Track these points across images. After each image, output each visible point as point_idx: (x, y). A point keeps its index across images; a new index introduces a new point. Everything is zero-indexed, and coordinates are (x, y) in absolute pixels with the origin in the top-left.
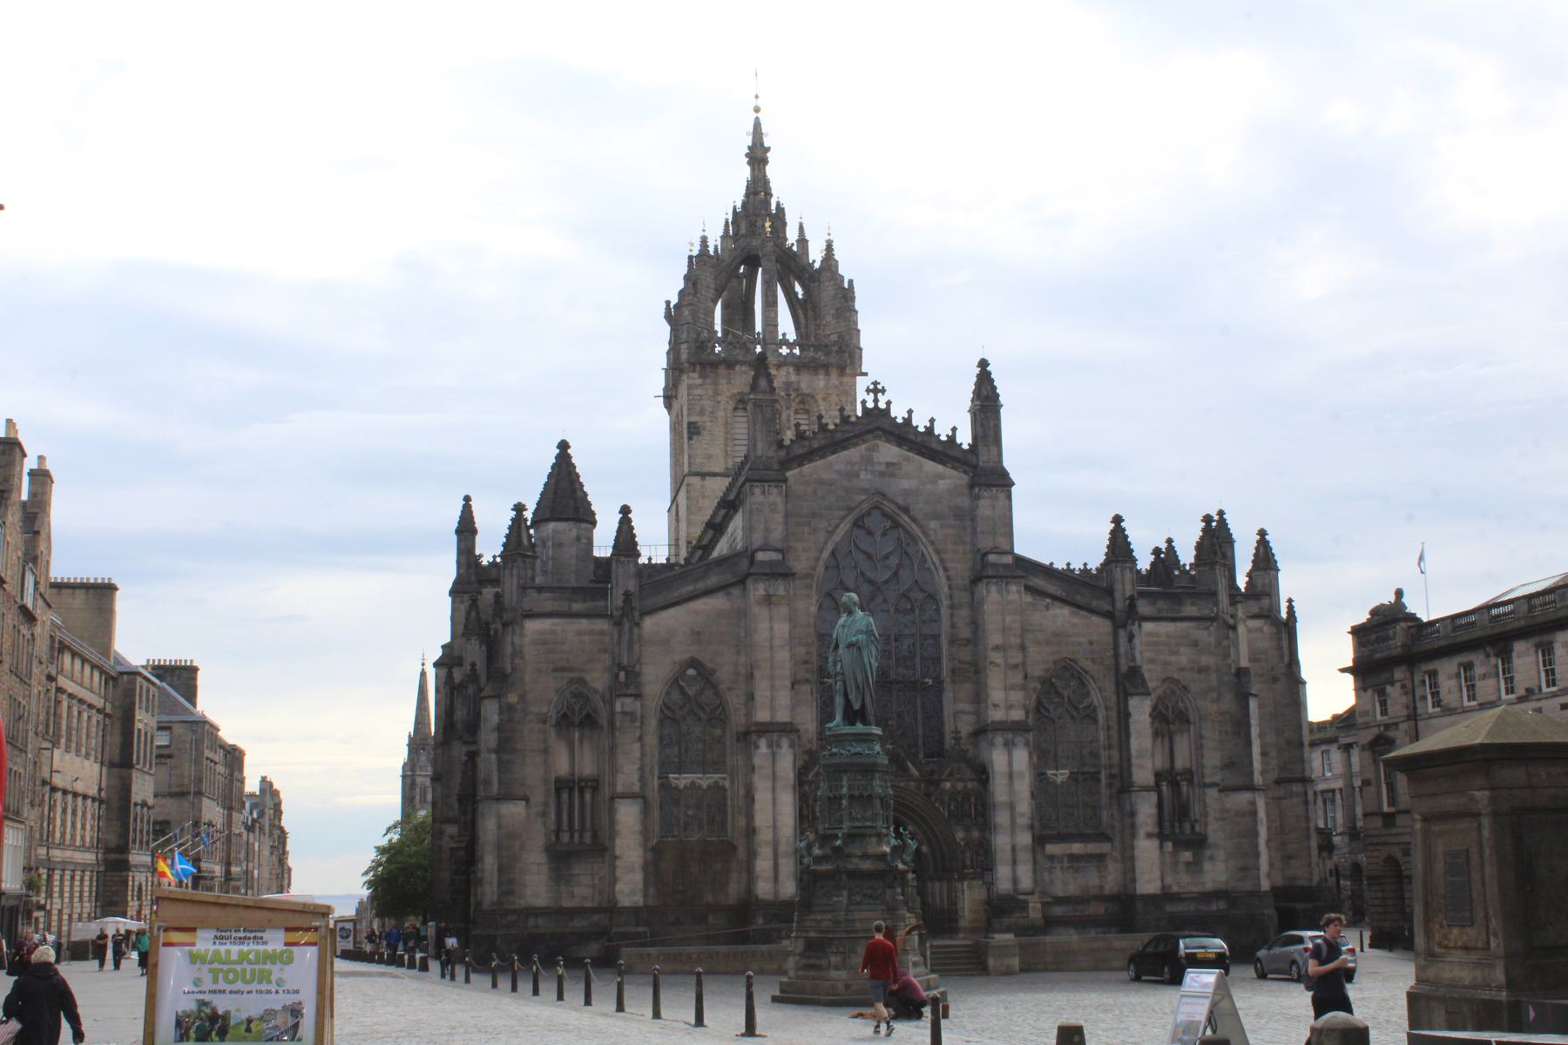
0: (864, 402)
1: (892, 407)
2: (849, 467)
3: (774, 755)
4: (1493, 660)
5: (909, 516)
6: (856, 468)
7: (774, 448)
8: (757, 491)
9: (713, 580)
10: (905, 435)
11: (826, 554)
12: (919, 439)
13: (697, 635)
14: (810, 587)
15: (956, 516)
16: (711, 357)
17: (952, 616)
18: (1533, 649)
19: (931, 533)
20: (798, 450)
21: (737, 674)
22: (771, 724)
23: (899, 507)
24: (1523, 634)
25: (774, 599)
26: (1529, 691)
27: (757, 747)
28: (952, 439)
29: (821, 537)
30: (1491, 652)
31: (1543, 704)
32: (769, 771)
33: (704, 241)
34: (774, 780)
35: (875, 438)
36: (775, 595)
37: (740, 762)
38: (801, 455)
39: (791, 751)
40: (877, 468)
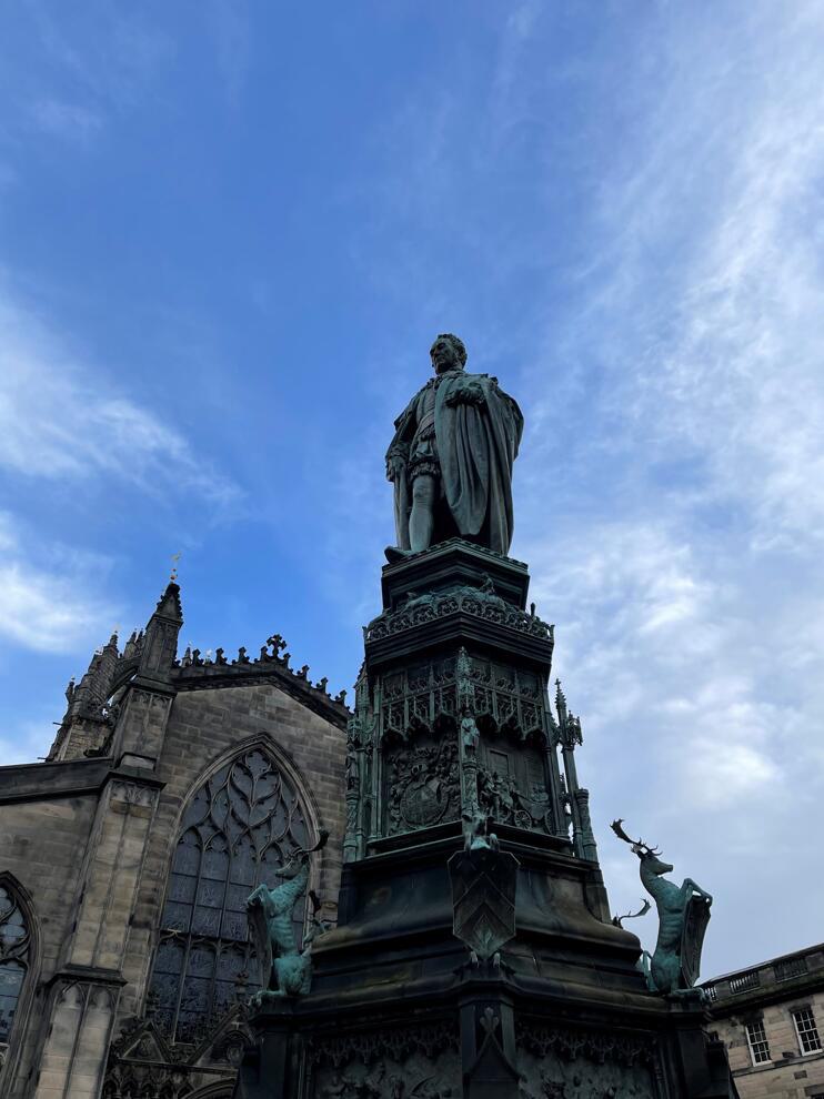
0: (264, 650)
1: (290, 660)
2: (240, 704)
3: (83, 1015)
4: (741, 1029)
5: (292, 763)
6: (247, 705)
7: (167, 665)
8: (141, 699)
9: (63, 784)
10: (296, 686)
11: (199, 783)
12: (311, 693)
13: (22, 845)
14: (175, 815)
15: (337, 773)
16: (98, 717)
17: (322, 875)
18: (787, 1015)
19: (311, 783)
20: (190, 673)
21: (62, 903)
22: (90, 968)
23: (284, 753)
24: (775, 1000)
25: (133, 809)
26: (788, 1058)
27: (62, 1000)
28: (340, 702)
29: (199, 762)
30: (738, 1022)
31: (805, 1067)
32: (70, 1038)
33: (115, 638)
34: (75, 1050)
35: (273, 683)
36: (135, 805)
37: (31, 1025)
38: (190, 679)
39: (108, 1011)
40: (267, 710)
